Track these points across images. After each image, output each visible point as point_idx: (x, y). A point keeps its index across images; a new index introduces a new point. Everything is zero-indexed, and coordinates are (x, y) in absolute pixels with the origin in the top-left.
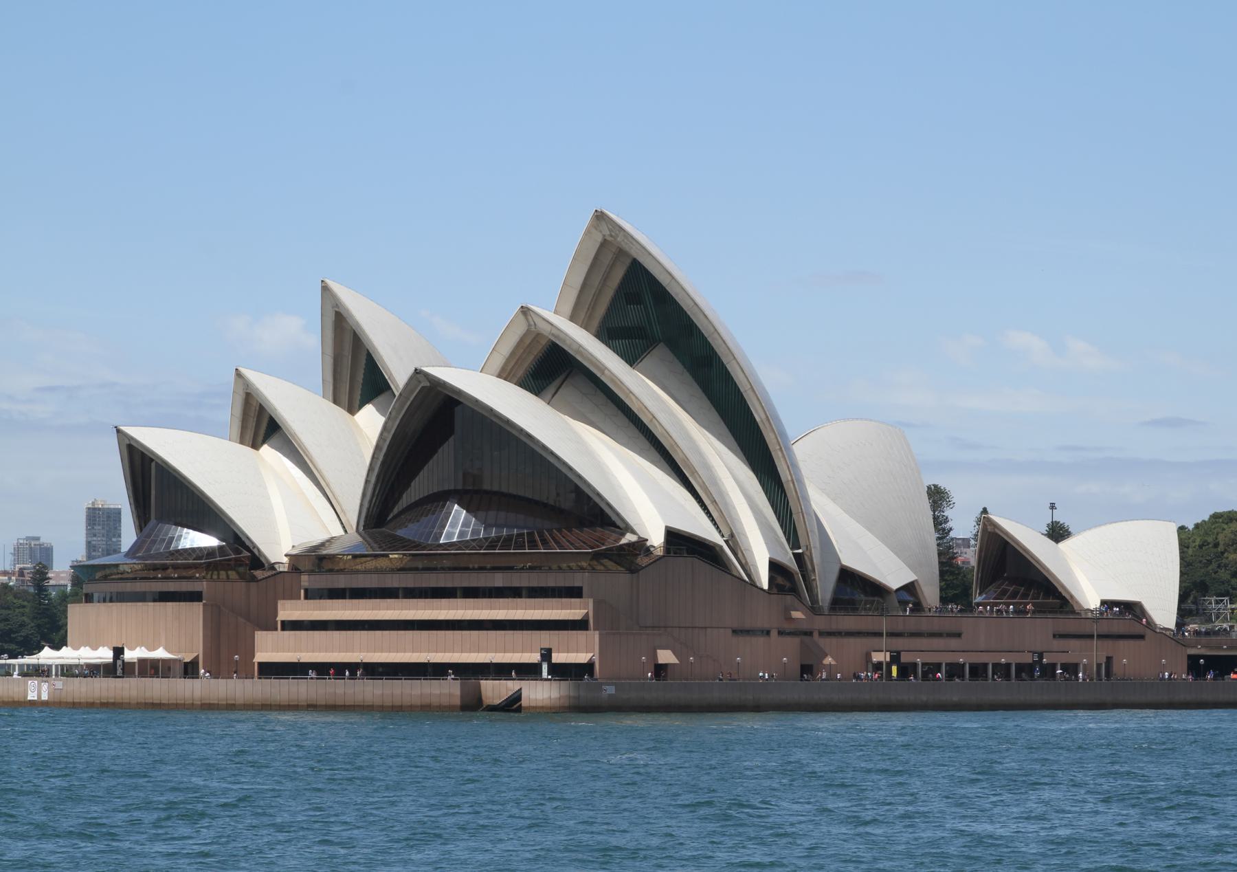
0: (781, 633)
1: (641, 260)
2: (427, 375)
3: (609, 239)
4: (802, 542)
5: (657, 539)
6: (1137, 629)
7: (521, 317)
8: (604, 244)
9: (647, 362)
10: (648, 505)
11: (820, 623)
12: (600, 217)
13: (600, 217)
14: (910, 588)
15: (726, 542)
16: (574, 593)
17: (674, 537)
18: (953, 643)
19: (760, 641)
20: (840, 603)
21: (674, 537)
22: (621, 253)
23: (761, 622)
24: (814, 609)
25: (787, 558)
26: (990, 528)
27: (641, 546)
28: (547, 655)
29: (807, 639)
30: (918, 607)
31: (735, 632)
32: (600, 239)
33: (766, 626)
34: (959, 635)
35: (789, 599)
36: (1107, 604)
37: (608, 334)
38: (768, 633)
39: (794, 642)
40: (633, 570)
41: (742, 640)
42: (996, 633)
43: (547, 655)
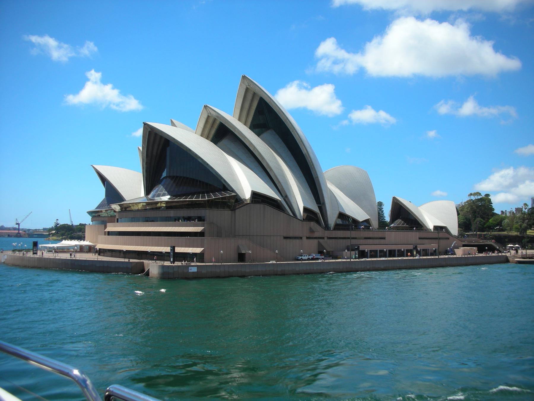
0: (307, 238)
1: (265, 98)
2: (148, 125)
3: (248, 87)
6: (447, 236)
7: (205, 110)
8: (247, 90)
9: (265, 135)
10: (244, 181)
11: (327, 234)
12: (244, 77)
13: (244, 77)
14: (367, 221)
15: (284, 200)
16: (201, 219)
17: (255, 195)
18: (382, 241)
19: (298, 241)
21: (255, 195)
22: (254, 94)
23: (297, 234)
24: (327, 227)
25: (314, 207)
26: (395, 201)
27: (238, 200)
28: (173, 248)
29: (321, 241)
31: (285, 238)
32: (245, 87)
33: (301, 235)
34: (384, 238)
35: (313, 224)
36: (436, 228)
37: (253, 127)
38: (301, 238)
39: (315, 242)
40: (233, 209)
41: (288, 240)
42: (398, 239)
43: (173, 248)
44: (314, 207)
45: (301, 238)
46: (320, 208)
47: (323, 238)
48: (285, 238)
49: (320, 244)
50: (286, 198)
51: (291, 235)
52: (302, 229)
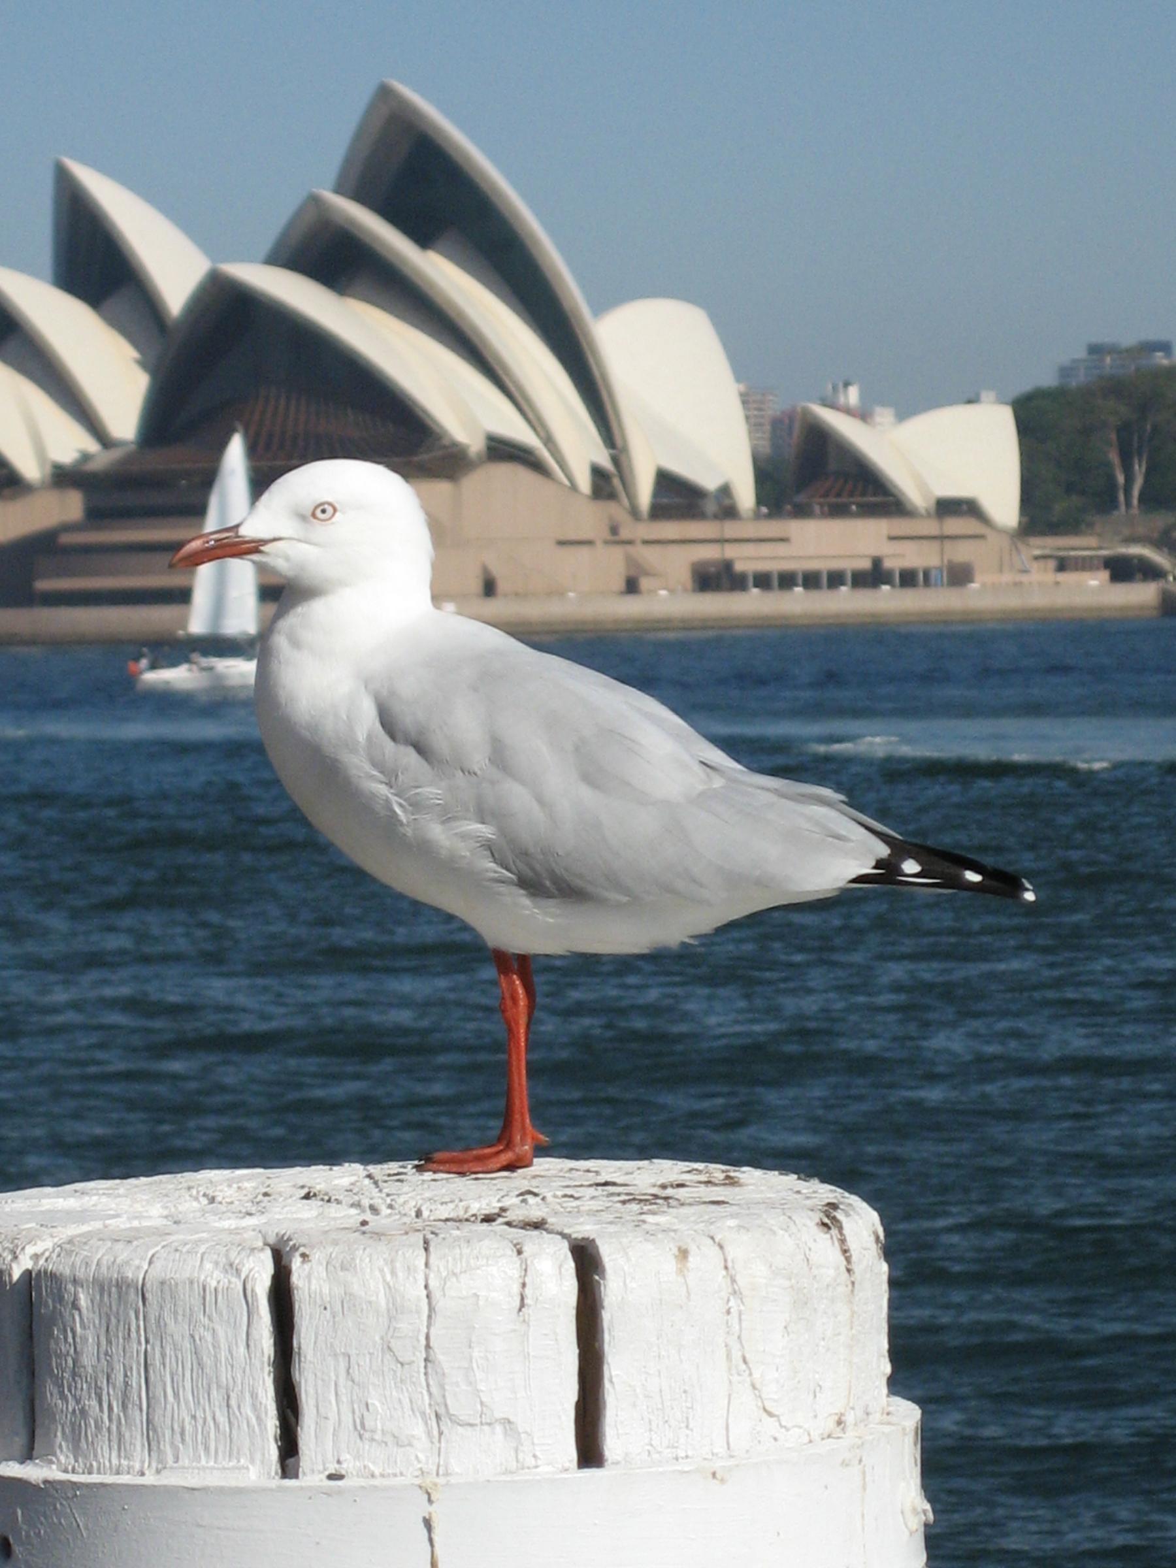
0: (606, 542)
4: (619, 442)
5: (474, 444)
15: (545, 445)
18: (781, 549)
20: (659, 512)
24: (634, 512)
25: (605, 462)
30: (729, 512)
31: (561, 543)
35: (611, 508)
44: (603, 459)
45: (589, 543)
46: (616, 461)
47: (630, 542)
48: (561, 543)
49: (630, 561)
50: (549, 440)
51: (572, 536)
52: (589, 518)
